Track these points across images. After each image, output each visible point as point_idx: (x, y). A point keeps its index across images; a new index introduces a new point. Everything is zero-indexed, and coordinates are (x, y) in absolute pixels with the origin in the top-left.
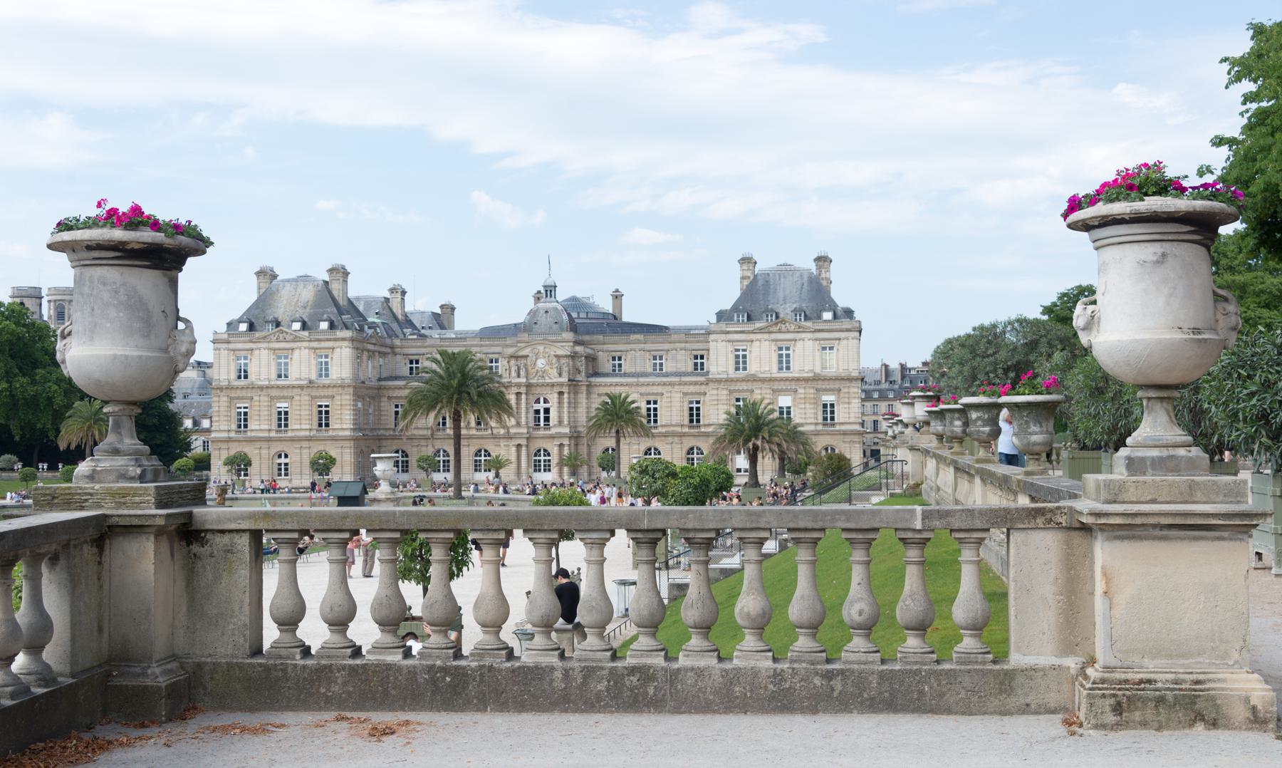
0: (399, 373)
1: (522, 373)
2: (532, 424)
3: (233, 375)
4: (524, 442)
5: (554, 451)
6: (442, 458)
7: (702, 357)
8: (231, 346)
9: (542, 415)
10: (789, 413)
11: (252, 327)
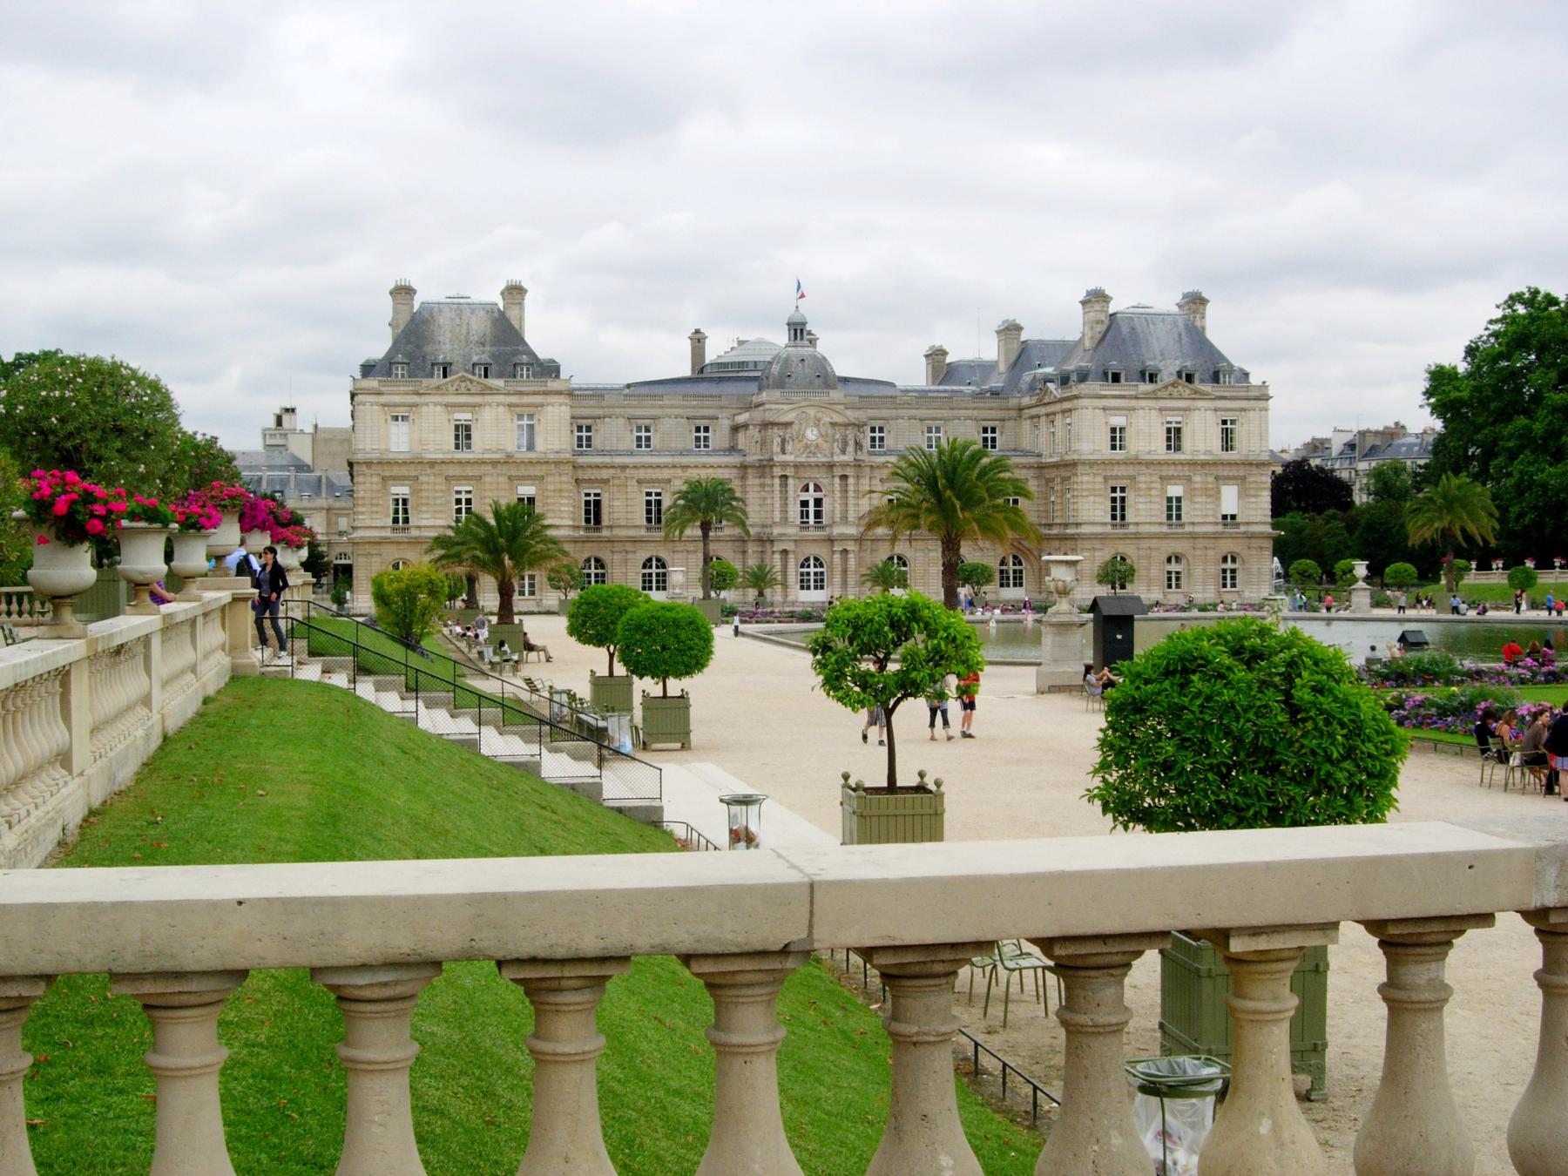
1: (789, 448)
2: (798, 521)
4: (790, 547)
6: (593, 571)
7: (993, 430)
8: (383, 399)
9: (811, 509)
10: (1179, 508)
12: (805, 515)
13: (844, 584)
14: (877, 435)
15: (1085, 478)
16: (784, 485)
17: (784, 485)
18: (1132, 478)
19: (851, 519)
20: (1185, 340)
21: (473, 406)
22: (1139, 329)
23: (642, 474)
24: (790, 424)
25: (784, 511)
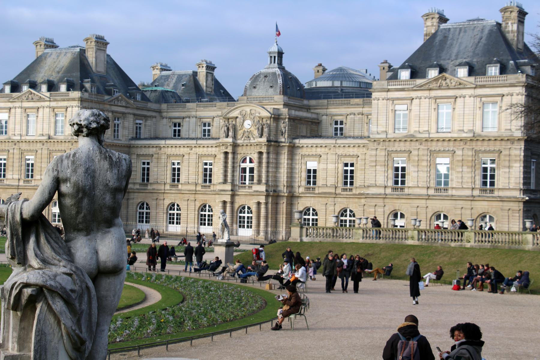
0: (164, 135)
1: (230, 134)
9: (248, 174)
13: (258, 225)
14: (339, 126)
15: (374, 152)
16: (226, 158)
17: (226, 158)
19: (264, 180)
22: (451, 36)
23: (169, 151)
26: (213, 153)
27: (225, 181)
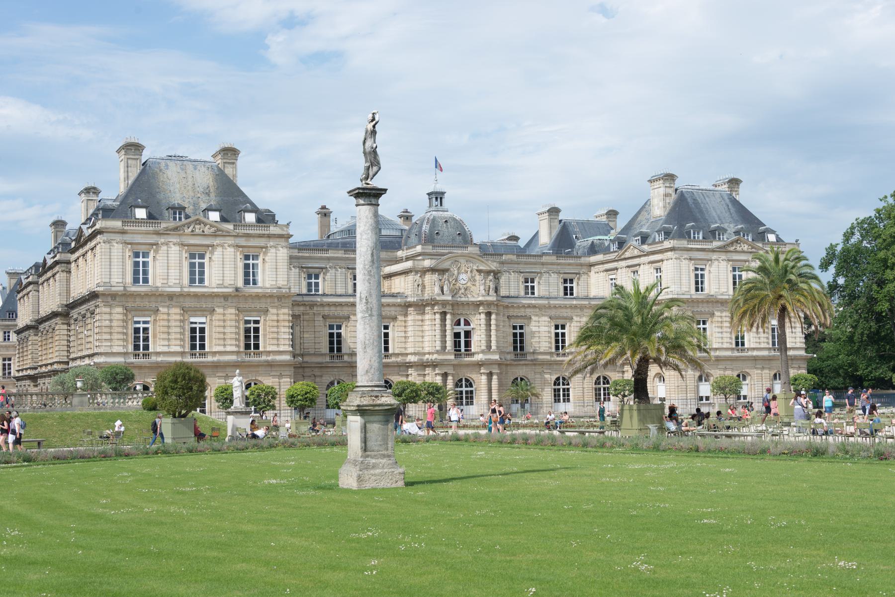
3: (129, 278)
4: (450, 371)
5: (480, 382)
7: (571, 281)
8: (128, 238)
9: (463, 339)
11: (150, 216)
12: (457, 344)
16: (443, 320)
17: (443, 320)
18: (713, 315)
19: (494, 347)
20: (733, 210)
21: (208, 246)
23: (326, 311)
24: (447, 270)
25: (444, 342)
26: (393, 313)
27: (444, 347)
